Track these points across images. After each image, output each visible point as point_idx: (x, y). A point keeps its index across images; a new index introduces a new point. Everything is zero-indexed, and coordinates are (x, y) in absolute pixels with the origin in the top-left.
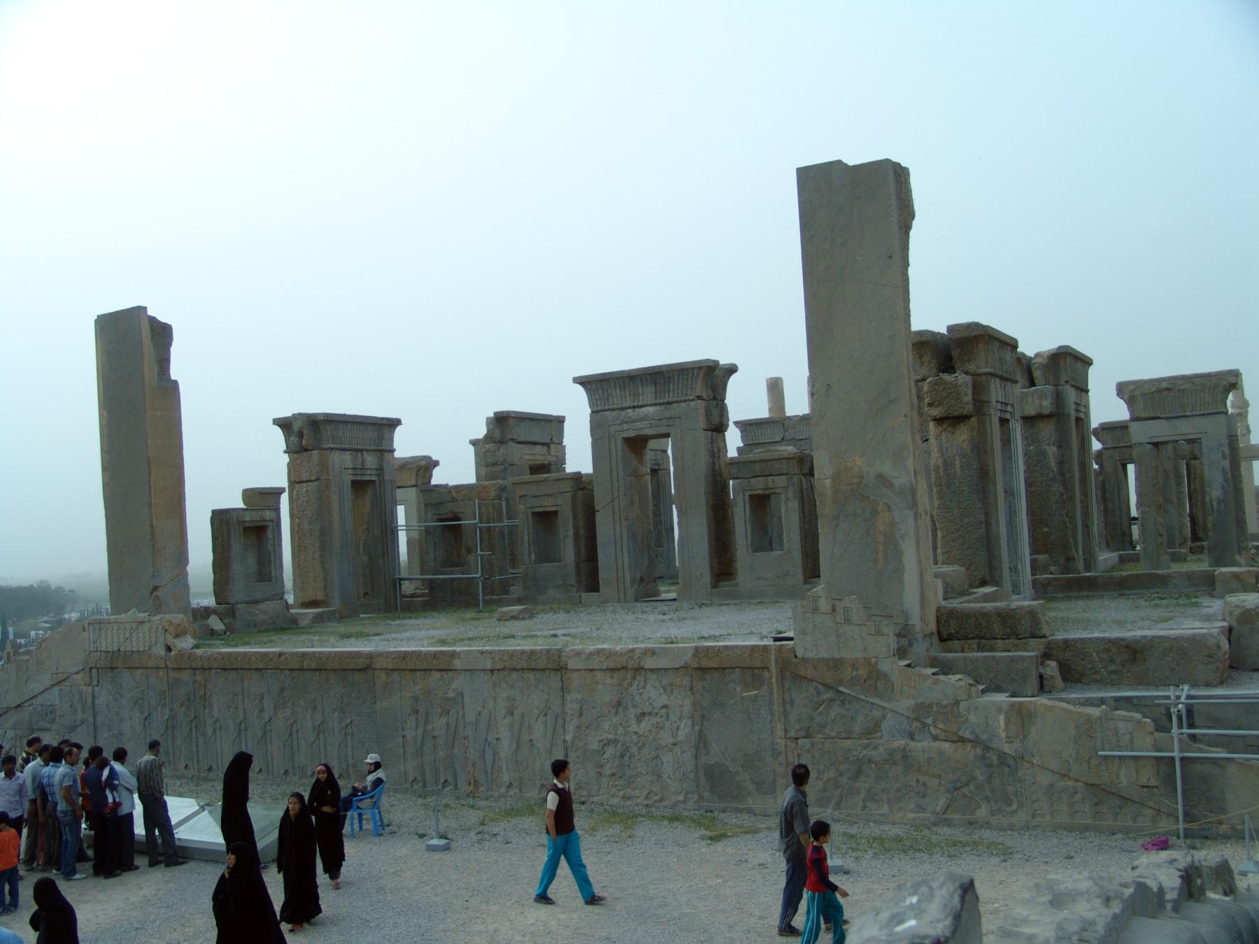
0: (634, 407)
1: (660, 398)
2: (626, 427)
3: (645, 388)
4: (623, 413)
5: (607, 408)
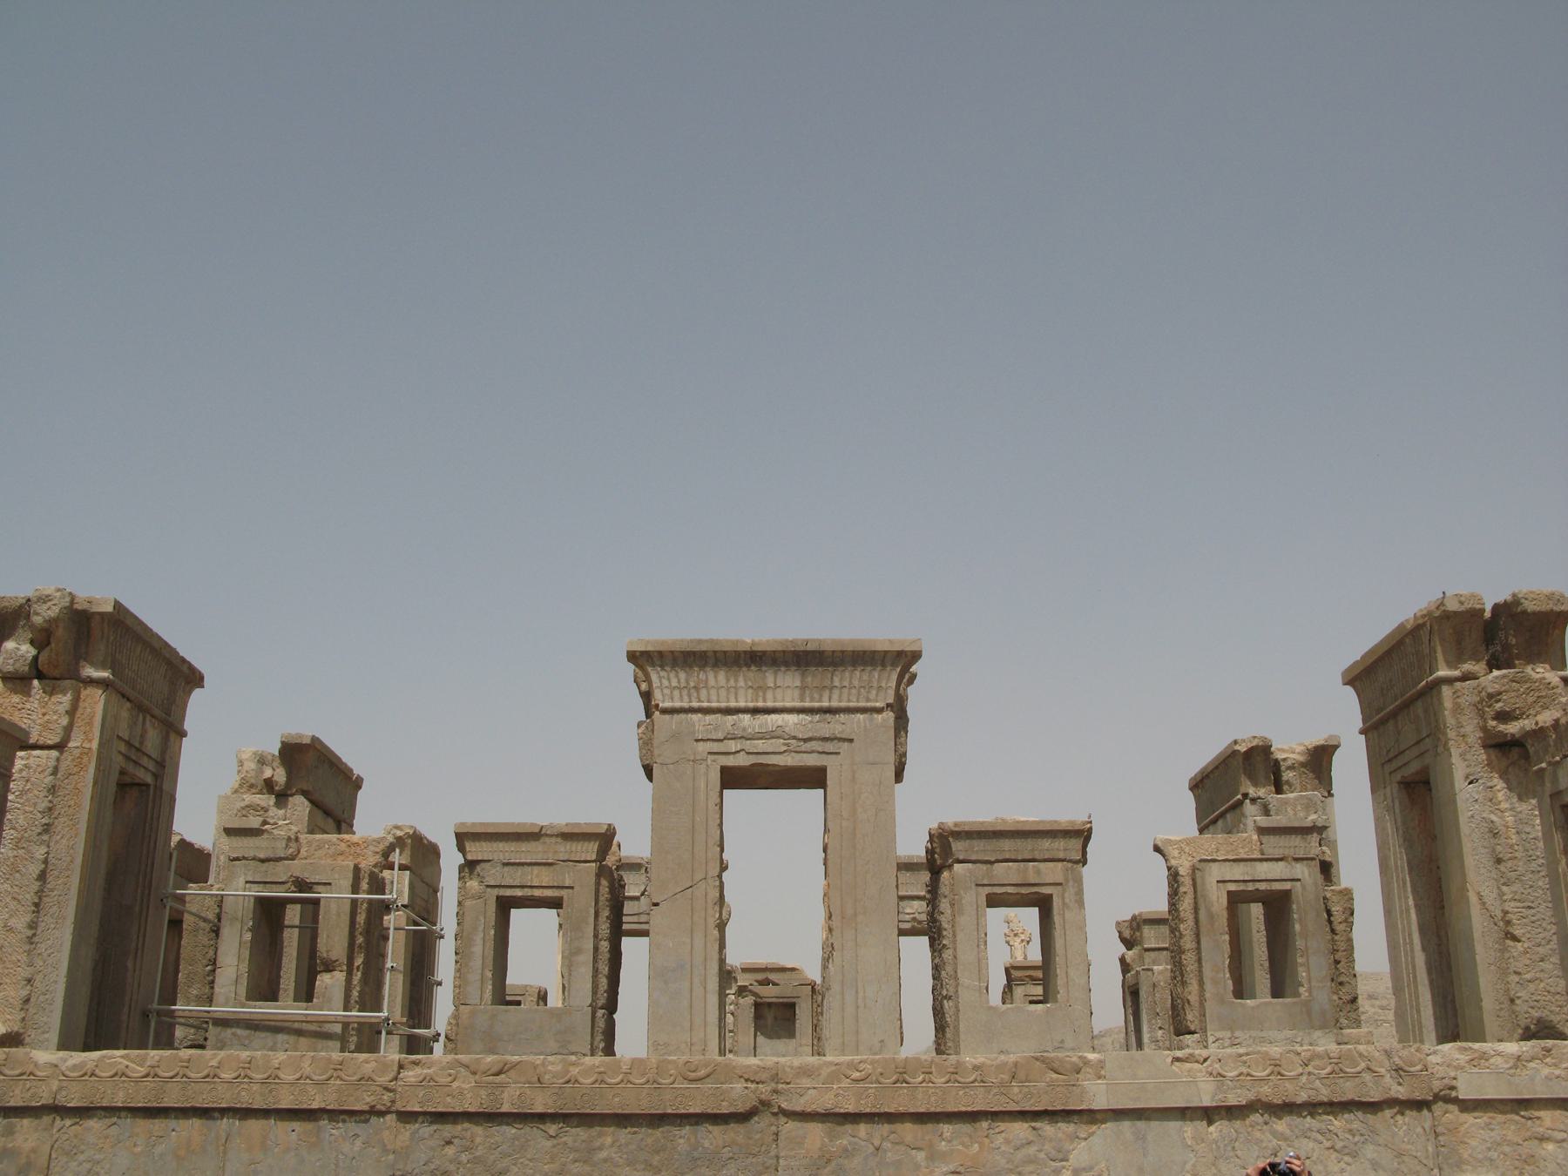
0: (755, 711)
1: (812, 700)
2: (733, 746)
5: (695, 704)
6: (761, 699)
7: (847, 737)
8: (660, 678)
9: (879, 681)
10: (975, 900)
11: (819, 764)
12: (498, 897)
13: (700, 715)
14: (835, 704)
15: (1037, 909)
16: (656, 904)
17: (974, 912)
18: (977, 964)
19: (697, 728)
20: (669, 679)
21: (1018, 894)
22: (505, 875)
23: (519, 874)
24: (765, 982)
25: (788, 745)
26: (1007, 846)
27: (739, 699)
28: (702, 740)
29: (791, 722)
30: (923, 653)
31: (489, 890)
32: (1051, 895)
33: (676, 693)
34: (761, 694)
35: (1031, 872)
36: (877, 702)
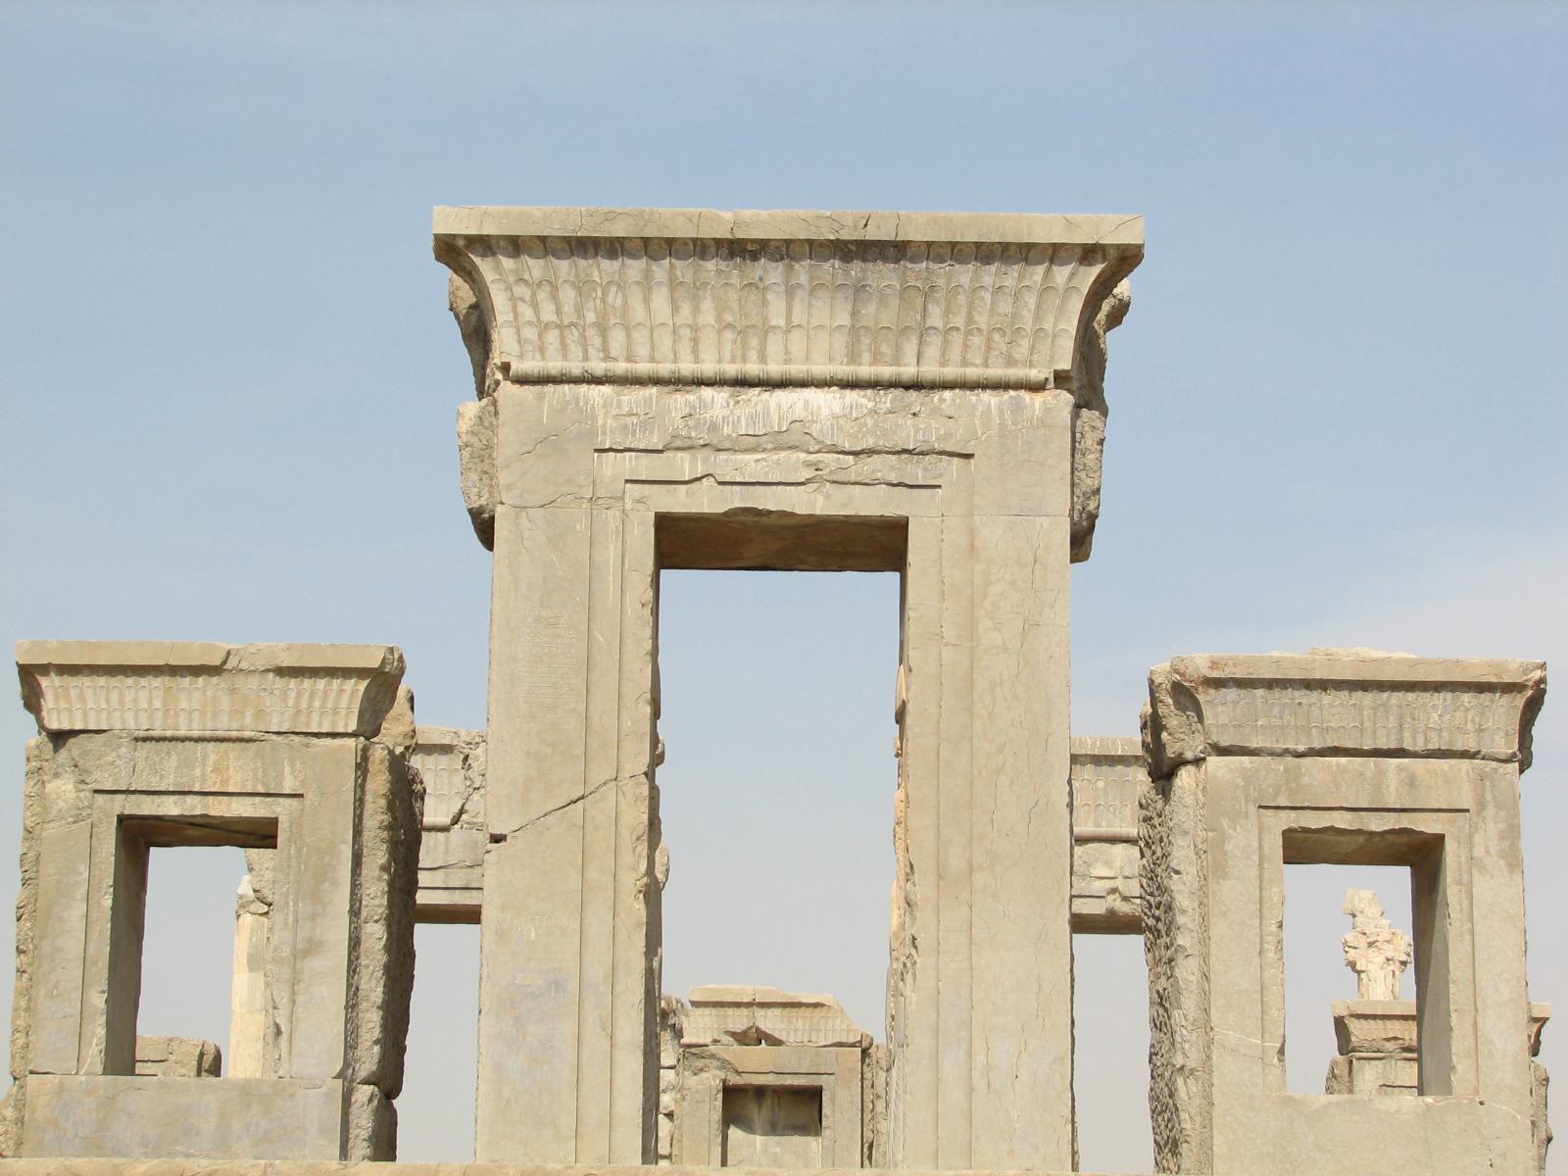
0: (742, 382)
2: (684, 465)
3: (800, 296)
4: (681, 401)
5: (598, 367)
6: (753, 355)
7: (958, 450)
8: (514, 301)
9: (1037, 318)
10: (1256, 844)
11: (890, 511)
12: (122, 819)
13: (607, 389)
14: (930, 370)
15: (1408, 869)
16: (497, 839)
17: (1254, 872)
18: (1258, 996)
19: (600, 422)
20: (535, 305)
21: (1359, 832)
22: (141, 765)
23: (174, 762)
24: (754, 1037)
25: (808, 464)
26: (1339, 718)
27: (702, 356)
28: (611, 450)
29: (825, 412)
30: (1146, 251)
31: (100, 798)
32: (1441, 838)
33: (552, 337)
34: (754, 342)
35: (1392, 780)
36: (1031, 366)
